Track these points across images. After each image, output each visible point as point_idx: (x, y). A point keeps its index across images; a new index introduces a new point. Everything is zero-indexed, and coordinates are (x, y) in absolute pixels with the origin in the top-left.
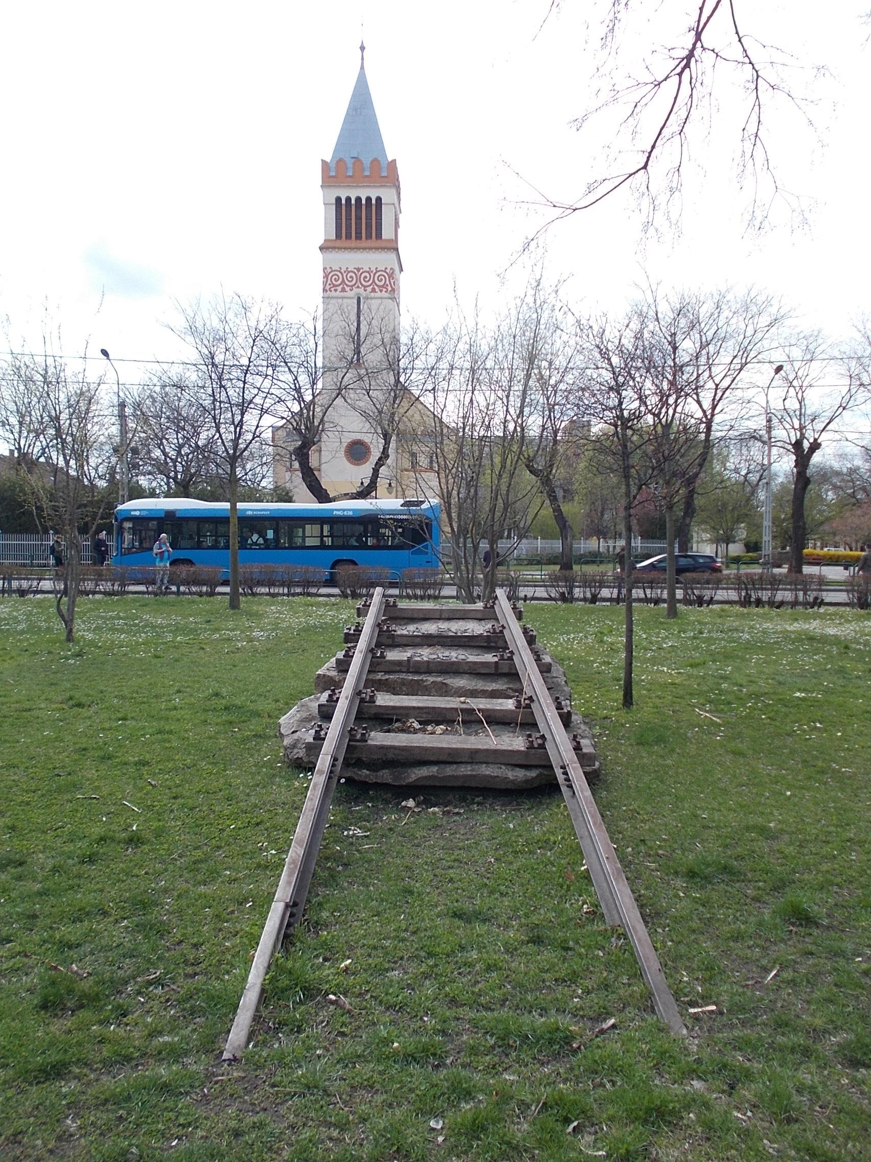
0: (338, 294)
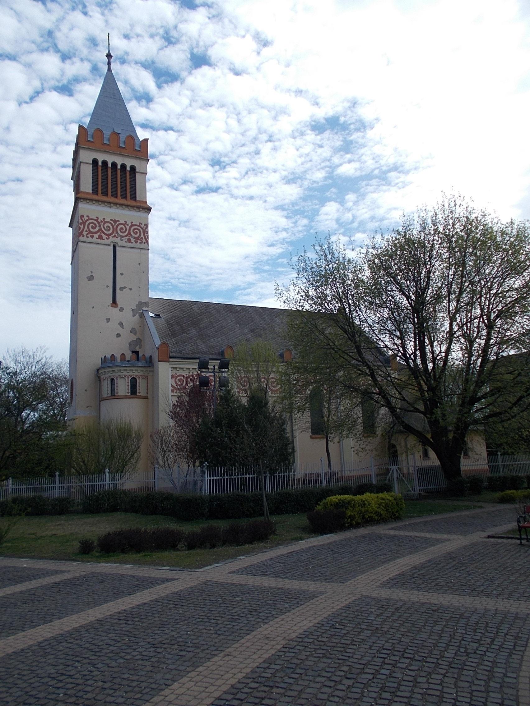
0: (94, 240)
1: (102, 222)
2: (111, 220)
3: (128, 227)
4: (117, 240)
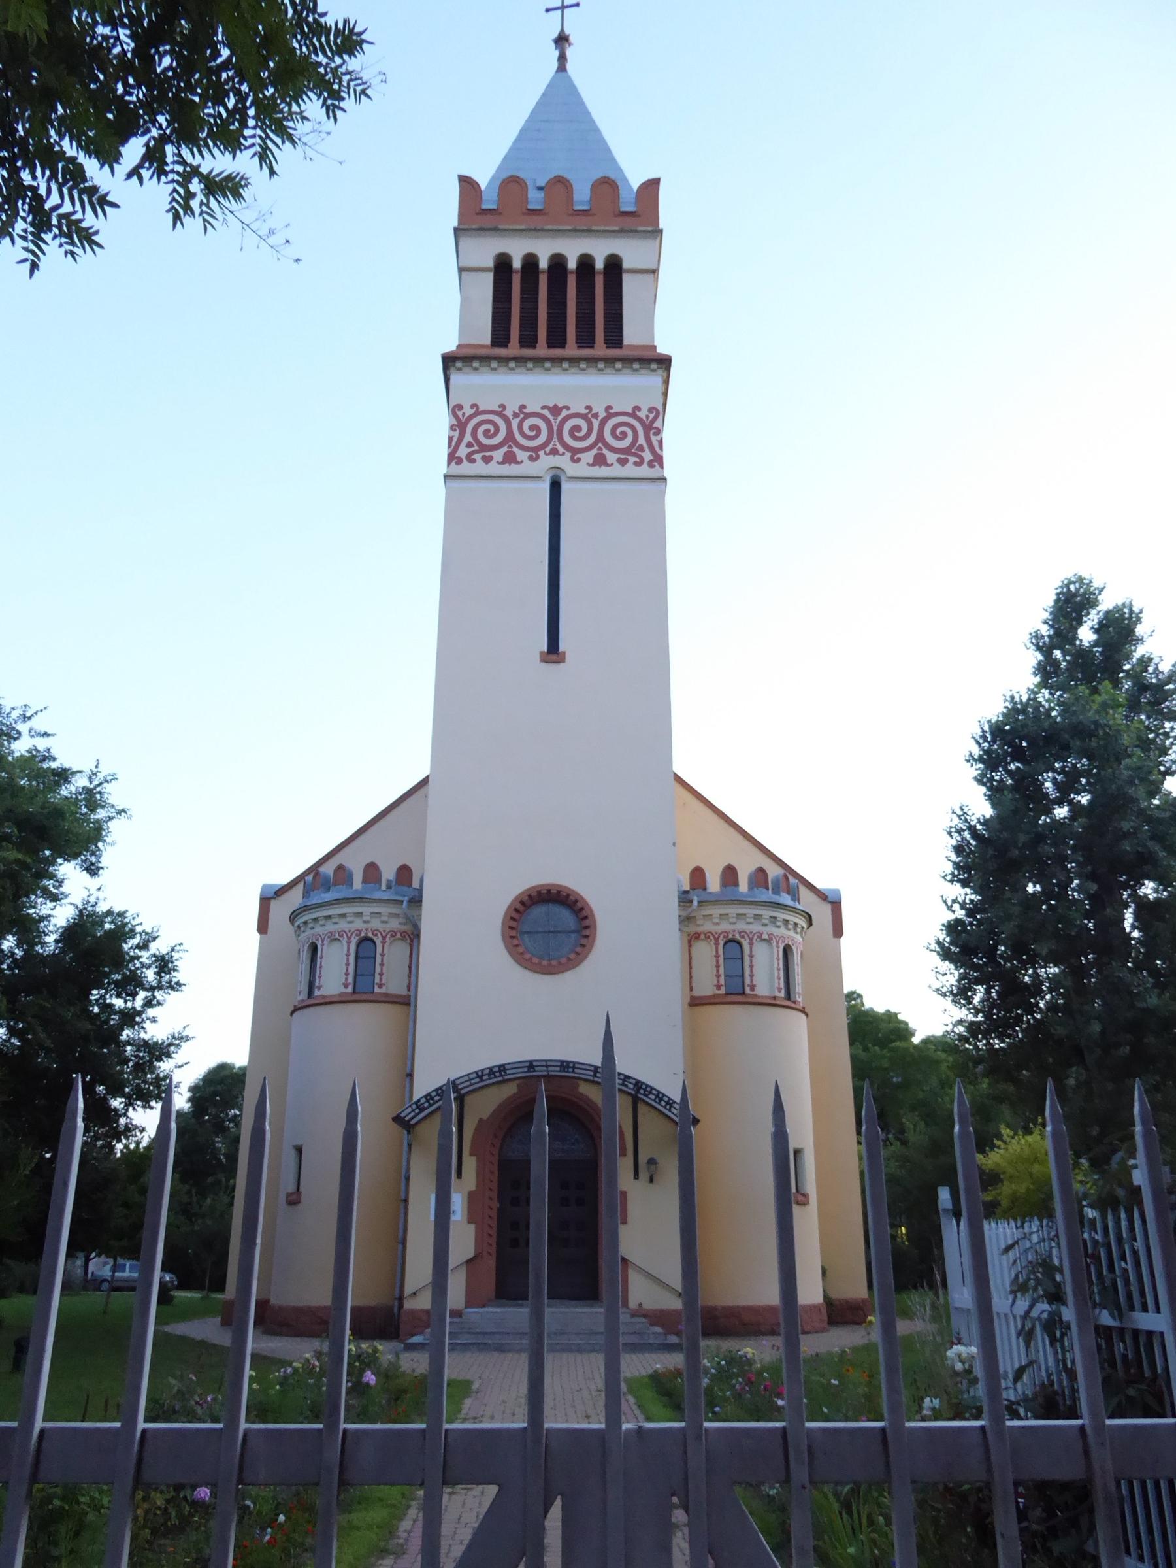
0: (493, 468)
3: (596, 424)
4: (563, 461)
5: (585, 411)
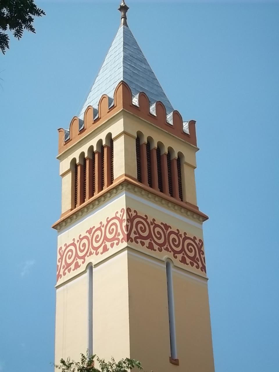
1: (152, 224)
2: (162, 223)
3: (181, 240)
4: (170, 255)
5: (177, 232)
